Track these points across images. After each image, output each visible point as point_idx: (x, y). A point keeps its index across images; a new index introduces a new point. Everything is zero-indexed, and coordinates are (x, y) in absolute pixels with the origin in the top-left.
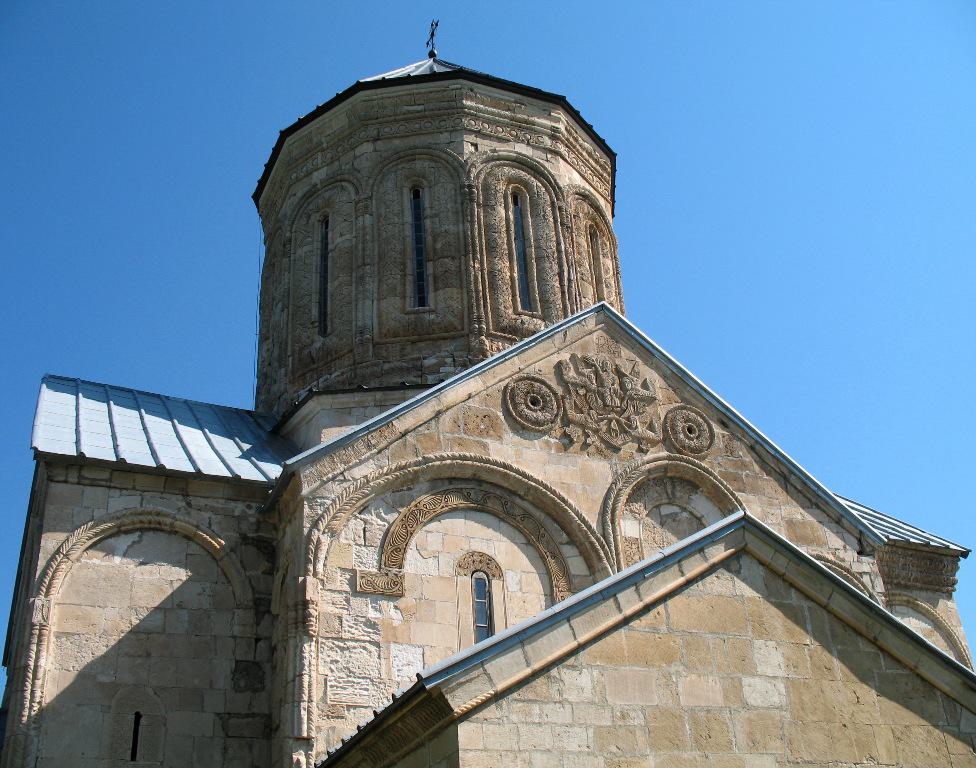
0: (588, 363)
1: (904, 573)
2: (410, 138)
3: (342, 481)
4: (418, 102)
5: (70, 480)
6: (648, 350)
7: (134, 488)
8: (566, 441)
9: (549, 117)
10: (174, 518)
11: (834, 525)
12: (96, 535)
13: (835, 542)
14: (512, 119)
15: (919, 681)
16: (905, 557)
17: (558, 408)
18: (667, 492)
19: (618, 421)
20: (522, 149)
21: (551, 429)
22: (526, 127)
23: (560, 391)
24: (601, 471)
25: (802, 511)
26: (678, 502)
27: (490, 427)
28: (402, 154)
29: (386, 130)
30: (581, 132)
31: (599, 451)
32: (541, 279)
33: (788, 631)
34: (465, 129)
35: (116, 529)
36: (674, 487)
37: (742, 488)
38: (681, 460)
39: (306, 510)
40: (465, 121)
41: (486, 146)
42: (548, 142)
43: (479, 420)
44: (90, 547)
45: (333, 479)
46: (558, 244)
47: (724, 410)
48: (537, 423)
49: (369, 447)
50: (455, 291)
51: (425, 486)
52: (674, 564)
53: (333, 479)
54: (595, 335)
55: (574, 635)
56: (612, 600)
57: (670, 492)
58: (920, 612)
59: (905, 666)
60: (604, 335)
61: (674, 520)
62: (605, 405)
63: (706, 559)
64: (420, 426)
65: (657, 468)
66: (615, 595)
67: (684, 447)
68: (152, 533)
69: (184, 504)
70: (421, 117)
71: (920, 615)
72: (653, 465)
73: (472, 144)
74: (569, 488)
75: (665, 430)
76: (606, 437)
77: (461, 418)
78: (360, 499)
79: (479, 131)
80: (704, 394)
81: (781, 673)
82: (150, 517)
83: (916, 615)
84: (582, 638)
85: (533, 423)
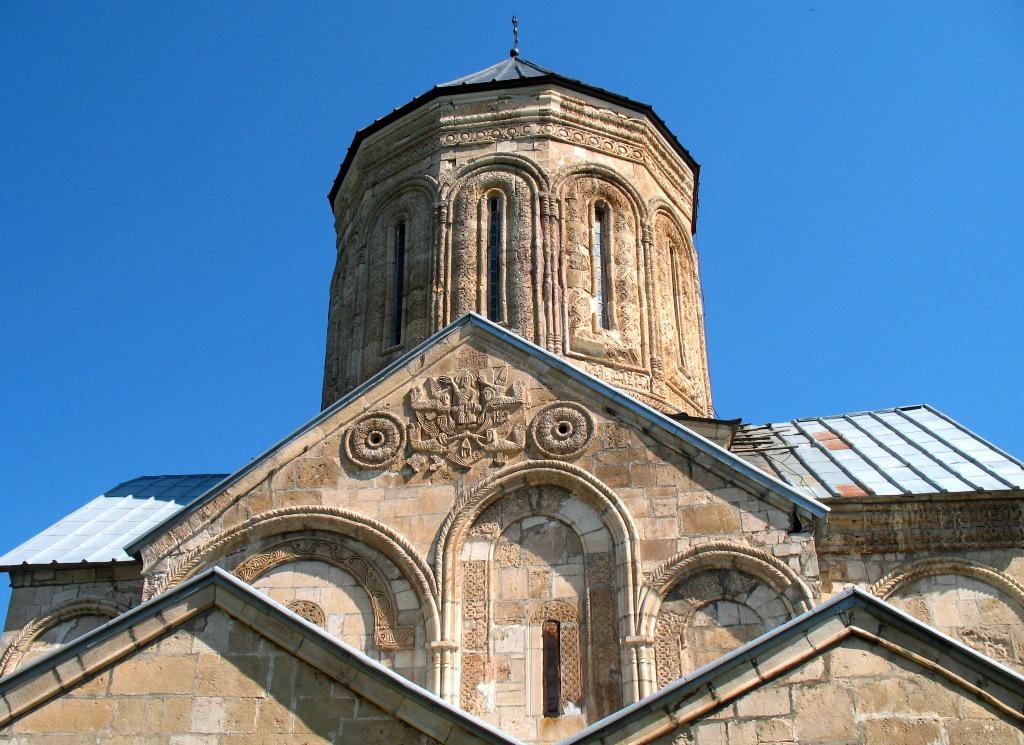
1: (947, 533)
3: (177, 555)
5: (25, 584)
7: (72, 583)
8: (409, 472)
9: (539, 102)
10: (100, 604)
11: (755, 503)
12: (40, 627)
13: (753, 523)
14: (494, 118)
15: (401, 727)
16: (947, 511)
17: (402, 438)
18: (531, 504)
19: (471, 439)
20: (506, 148)
21: (392, 463)
22: (514, 121)
23: (404, 422)
24: (443, 494)
25: (709, 494)
26: (543, 512)
27: (324, 474)
28: (391, 193)
30: (585, 99)
31: (445, 476)
32: (511, 284)
33: (242, 685)
35: (56, 620)
36: (540, 496)
37: (625, 481)
38: (551, 466)
39: (146, 585)
40: (443, 140)
41: (463, 158)
42: (535, 129)
44: (36, 639)
45: (170, 554)
46: (534, 239)
47: (611, 396)
48: (375, 460)
49: (203, 518)
50: (420, 321)
51: (258, 545)
52: (124, 631)
53: (170, 554)
54: (458, 351)
55: (9, 708)
56: (51, 673)
57: (534, 503)
58: (978, 580)
59: (386, 713)
60: (469, 347)
61: (538, 533)
62: (458, 424)
63: (163, 621)
64: (253, 489)
66: (54, 668)
67: (551, 450)
68: (85, 619)
69: (112, 589)
70: (409, 148)
71: (978, 584)
73: (450, 161)
74: (398, 520)
75: (529, 436)
76: (455, 459)
78: (190, 569)
81: (217, 729)
82: (81, 606)
83: (970, 583)
84: (15, 711)
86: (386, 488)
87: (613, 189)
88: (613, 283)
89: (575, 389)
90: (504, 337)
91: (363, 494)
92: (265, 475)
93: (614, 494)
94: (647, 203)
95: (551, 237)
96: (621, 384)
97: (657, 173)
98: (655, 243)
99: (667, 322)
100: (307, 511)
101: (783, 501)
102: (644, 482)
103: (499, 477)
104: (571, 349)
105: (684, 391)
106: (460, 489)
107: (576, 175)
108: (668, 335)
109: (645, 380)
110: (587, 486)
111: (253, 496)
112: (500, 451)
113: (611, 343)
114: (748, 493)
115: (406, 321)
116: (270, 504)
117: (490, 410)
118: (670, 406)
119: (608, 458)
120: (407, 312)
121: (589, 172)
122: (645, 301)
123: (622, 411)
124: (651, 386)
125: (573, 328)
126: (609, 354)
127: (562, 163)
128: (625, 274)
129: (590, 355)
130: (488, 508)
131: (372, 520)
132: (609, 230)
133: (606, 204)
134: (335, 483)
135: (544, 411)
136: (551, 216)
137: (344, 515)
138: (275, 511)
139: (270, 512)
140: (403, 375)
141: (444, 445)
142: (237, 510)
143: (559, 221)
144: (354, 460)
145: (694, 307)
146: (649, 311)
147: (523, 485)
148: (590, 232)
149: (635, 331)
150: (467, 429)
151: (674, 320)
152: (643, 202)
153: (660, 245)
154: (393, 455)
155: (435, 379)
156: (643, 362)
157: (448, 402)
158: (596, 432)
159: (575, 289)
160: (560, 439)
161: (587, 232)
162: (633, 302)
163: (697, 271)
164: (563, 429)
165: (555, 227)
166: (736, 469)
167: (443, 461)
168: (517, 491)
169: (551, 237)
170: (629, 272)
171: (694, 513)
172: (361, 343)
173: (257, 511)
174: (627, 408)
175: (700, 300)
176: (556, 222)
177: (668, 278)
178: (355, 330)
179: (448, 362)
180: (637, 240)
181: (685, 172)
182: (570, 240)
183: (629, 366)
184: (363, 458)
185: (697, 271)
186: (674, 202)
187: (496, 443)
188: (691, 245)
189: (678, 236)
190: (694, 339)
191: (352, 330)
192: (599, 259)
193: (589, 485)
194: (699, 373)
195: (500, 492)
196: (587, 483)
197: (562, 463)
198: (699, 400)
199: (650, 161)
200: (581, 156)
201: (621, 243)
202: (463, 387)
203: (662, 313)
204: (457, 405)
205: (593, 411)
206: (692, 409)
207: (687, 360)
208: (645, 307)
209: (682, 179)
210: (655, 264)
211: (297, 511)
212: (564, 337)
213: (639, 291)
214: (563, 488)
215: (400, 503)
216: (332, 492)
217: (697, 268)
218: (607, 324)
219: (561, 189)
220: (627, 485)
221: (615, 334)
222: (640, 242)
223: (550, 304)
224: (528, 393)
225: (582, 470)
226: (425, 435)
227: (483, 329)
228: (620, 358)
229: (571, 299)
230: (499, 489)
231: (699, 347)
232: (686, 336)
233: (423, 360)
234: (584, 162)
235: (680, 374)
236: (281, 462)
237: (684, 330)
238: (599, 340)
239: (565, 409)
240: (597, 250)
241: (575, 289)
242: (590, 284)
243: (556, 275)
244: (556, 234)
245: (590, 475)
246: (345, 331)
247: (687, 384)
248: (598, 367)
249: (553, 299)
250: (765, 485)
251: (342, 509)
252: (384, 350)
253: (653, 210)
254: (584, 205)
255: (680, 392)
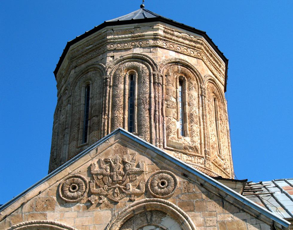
0: (106, 161)
2: (88, 62)
4: (90, 44)
6: (143, 146)
9: (153, 29)
11: (254, 220)
14: (133, 37)
17: (86, 188)
18: (147, 220)
19: (119, 188)
20: (138, 51)
21: (81, 199)
22: (141, 38)
23: (87, 180)
25: (232, 216)
27: (49, 205)
29: (79, 61)
30: (174, 28)
31: (107, 206)
32: (139, 115)
34: (108, 50)
36: (152, 216)
38: (157, 201)
40: (108, 47)
41: (118, 56)
42: (151, 42)
43: (43, 203)
46: (150, 94)
47: (185, 168)
48: (73, 198)
50: (96, 132)
54: (114, 146)
57: (149, 219)
60: (119, 145)
62: (113, 181)
64: (13, 212)
65: (138, 209)
67: (157, 194)
70: (92, 50)
72: (135, 207)
73: (111, 57)
75: (147, 187)
77: (34, 204)
79: (115, 49)
80: (174, 162)
85: (71, 199)
86: (78, 212)
87: (188, 71)
88: (187, 115)
89: (169, 165)
90: (135, 140)
91: (67, 215)
92: (19, 205)
93: (187, 215)
94: (203, 77)
95: (158, 93)
96: (190, 162)
97: (208, 63)
98: (207, 96)
99: (212, 133)
100: (40, 223)
101: (268, 219)
102: (201, 209)
103: (132, 206)
104: (167, 146)
105: (220, 165)
106: (113, 212)
107: (170, 64)
108: (213, 139)
109: (202, 161)
110: (174, 211)
111: (13, 216)
112: (133, 194)
113: (186, 143)
114: (251, 215)
115: (90, 132)
116: (22, 219)
117: (129, 174)
118: (213, 173)
119: (184, 198)
120: (90, 128)
121: (176, 63)
122: (202, 123)
123: (191, 175)
124: (205, 163)
125: (168, 135)
126: (185, 148)
127: (164, 58)
128: (193, 111)
129: (176, 149)
130: (127, 221)
131: (71, 227)
132: (185, 90)
133: (184, 78)
134: (54, 209)
135: (154, 175)
136: (158, 83)
137: (58, 225)
138: (24, 223)
139: (21, 223)
140: (87, 157)
141: (107, 191)
142: (5, 222)
143: (162, 85)
144: (63, 198)
145: (225, 126)
146: (204, 128)
147: (143, 210)
148: (177, 91)
149: (197, 137)
150: (117, 183)
151: (216, 132)
152: (201, 77)
153: (209, 97)
154: (82, 195)
155: (103, 159)
156: (201, 152)
157: (108, 170)
158: (178, 185)
159: (169, 117)
160: (161, 188)
161: (175, 91)
162: (196, 124)
163: (226, 110)
164: (163, 183)
165: (160, 88)
166: (245, 204)
167: (106, 199)
168: (140, 213)
169: (158, 93)
170: (195, 110)
171: (225, 224)
172: (68, 142)
173: (15, 223)
174: (192, 174)
175: (228, 123)
176: (160, 86)
177: (213, 113)
178: (65, 135)
179: (109, 151)
180: (198, 95)
181: (221, 63)
182: (167, 94)
183: (194, 154)
184: (68, 197)
185: (226, 110)
186: (216, 77)
187: (131, 190)
188: (224, 97)
189: (218, 93)
190: (225, 141)
191: (64, 135)
192: (180, 103)
193: (175, 210)
194: (227, 157)
195: (132, 214)
196: (174, 209)
197: (162, 200)
198: (228, 170)
199: (205, 58)
200: (173, 55)
201: (191, 96)
202: (116, 163)
203: (210, 129)
204: (113, 172)
205: (177, 175)
206: (224, 175)
207: (222, 152)
208: (202, 126)
209: (220, 66)
210: (207, 106)
211: (35, 223)
212: (164, 140)
213: (199, 119)
214: (163, 212)
215: (84, 219)
216: (52, 213)
217: (226, 108)
218: (184, 134)
219: (163, 71)
220: (193, 211)
221: (188, 139)
222: (200, 96)
223: (157, 124)
224: (146, 166)
225: (172, 203)
226: (97, 186)
227: (126, 136)
228: (190, 150)
229: (167, 123)
230: (132, 212)
231: (227, 145)
232: (221, 140)
233: (97, 150)
234: (174, 58)
235: (218, 158)
236: (28, 199)
237: (220, 137)
238: (180, 142)
239: (164, 174)
240: (179, 99)
241: (169, 117)
242: (176, 115)
243: (160, 111)
244: (160, 92)
245: (175, 206)
246: (61, 136)
247: (222, 162)
248: (180, 154)
249: (159, 122)
250: (259, 212)
251: (56, 222)
252: (79, 145)
253: (206, 80)
254: (174, 78)
255: (219, 166)
